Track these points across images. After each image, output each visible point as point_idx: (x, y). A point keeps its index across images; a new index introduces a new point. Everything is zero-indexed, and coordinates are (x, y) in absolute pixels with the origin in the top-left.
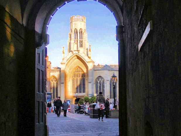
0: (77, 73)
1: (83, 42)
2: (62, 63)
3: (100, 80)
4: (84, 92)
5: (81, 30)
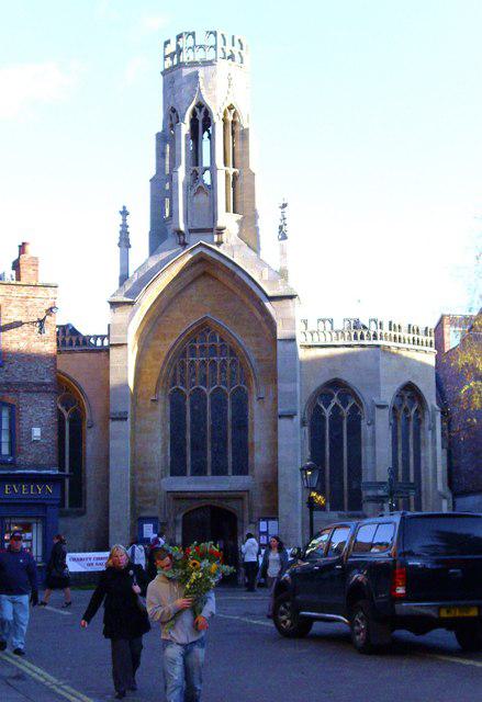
0: (198, 360)
1: (239, 182)
3: (335, 401)
4: (242, 468)
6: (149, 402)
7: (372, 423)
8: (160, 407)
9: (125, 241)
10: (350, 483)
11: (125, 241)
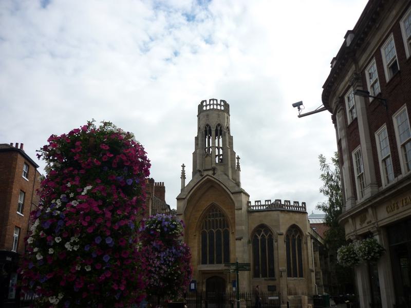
3: (263, 233)
4: (227, 260)
5: (219, 128)
7: (277, 241)
8: (197, 237)
9: (183, 177)
10: (269, 266)
11: (183, 177)
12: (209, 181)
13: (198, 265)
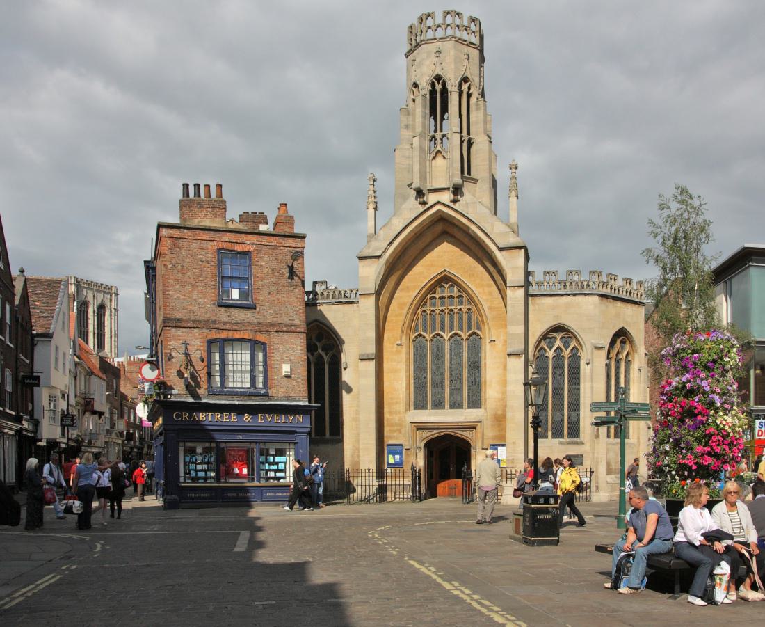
0: (438, 309)
2: (361, 255)
3: (558, 343)
4: (475, 402)
6: (396, 346)
8: (404, 350)
12: (441, 219)
13: (407, 410)
